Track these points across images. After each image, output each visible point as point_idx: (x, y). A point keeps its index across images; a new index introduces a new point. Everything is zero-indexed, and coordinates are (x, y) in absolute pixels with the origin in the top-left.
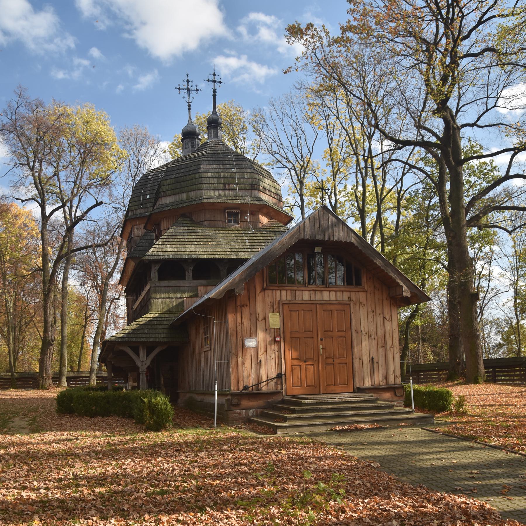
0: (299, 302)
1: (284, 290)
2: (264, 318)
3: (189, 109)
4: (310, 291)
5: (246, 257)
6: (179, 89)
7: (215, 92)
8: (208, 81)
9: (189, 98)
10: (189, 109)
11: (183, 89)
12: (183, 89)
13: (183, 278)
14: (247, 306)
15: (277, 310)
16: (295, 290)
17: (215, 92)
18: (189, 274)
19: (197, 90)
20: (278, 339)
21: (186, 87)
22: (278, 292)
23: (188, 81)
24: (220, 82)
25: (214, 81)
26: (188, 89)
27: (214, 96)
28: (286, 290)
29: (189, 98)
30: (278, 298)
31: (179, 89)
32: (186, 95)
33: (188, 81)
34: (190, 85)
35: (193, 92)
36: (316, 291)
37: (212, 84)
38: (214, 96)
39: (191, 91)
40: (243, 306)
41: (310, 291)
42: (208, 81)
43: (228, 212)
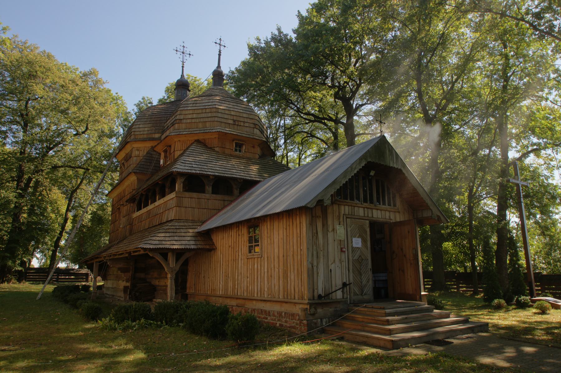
0: (356, 217)
1: (347, 205)
2: (333, 230)
3: (183, 67)
4: (364, 208)
5: (258, 179)
6: (177, 51)
7: (220, 52)
8: (216, 43)
9: (183, 58)
10: (183, 67)
11: (179, 51)
12: (179, 51)
13: (203, 191)
14: (320, 217)
15: (342, 223)
16: (354, 206)
17: (220, 52)
18: (209, 189)
19: (190, 55)
20: (344, 250)
21: (182, 51)
22: (342, 207)
23: (184, 47)
24: (225, 47)
25: (220, 45)
26: (183, 53)
27: (220, 55)
28: (348, 206)
29: (183, 58)
30: (343, 212)
31: (177, 51)
32: (181, 57)
33: (184, 47)
34: (185, 50)
35: (187, 55)
36: (368, 208)
37: (218, 45)
38: (220, 55)
39: (185, 55)
40: (318, 217)
41: (364, 208)
42: (216, 43)
43: (236, 143)
